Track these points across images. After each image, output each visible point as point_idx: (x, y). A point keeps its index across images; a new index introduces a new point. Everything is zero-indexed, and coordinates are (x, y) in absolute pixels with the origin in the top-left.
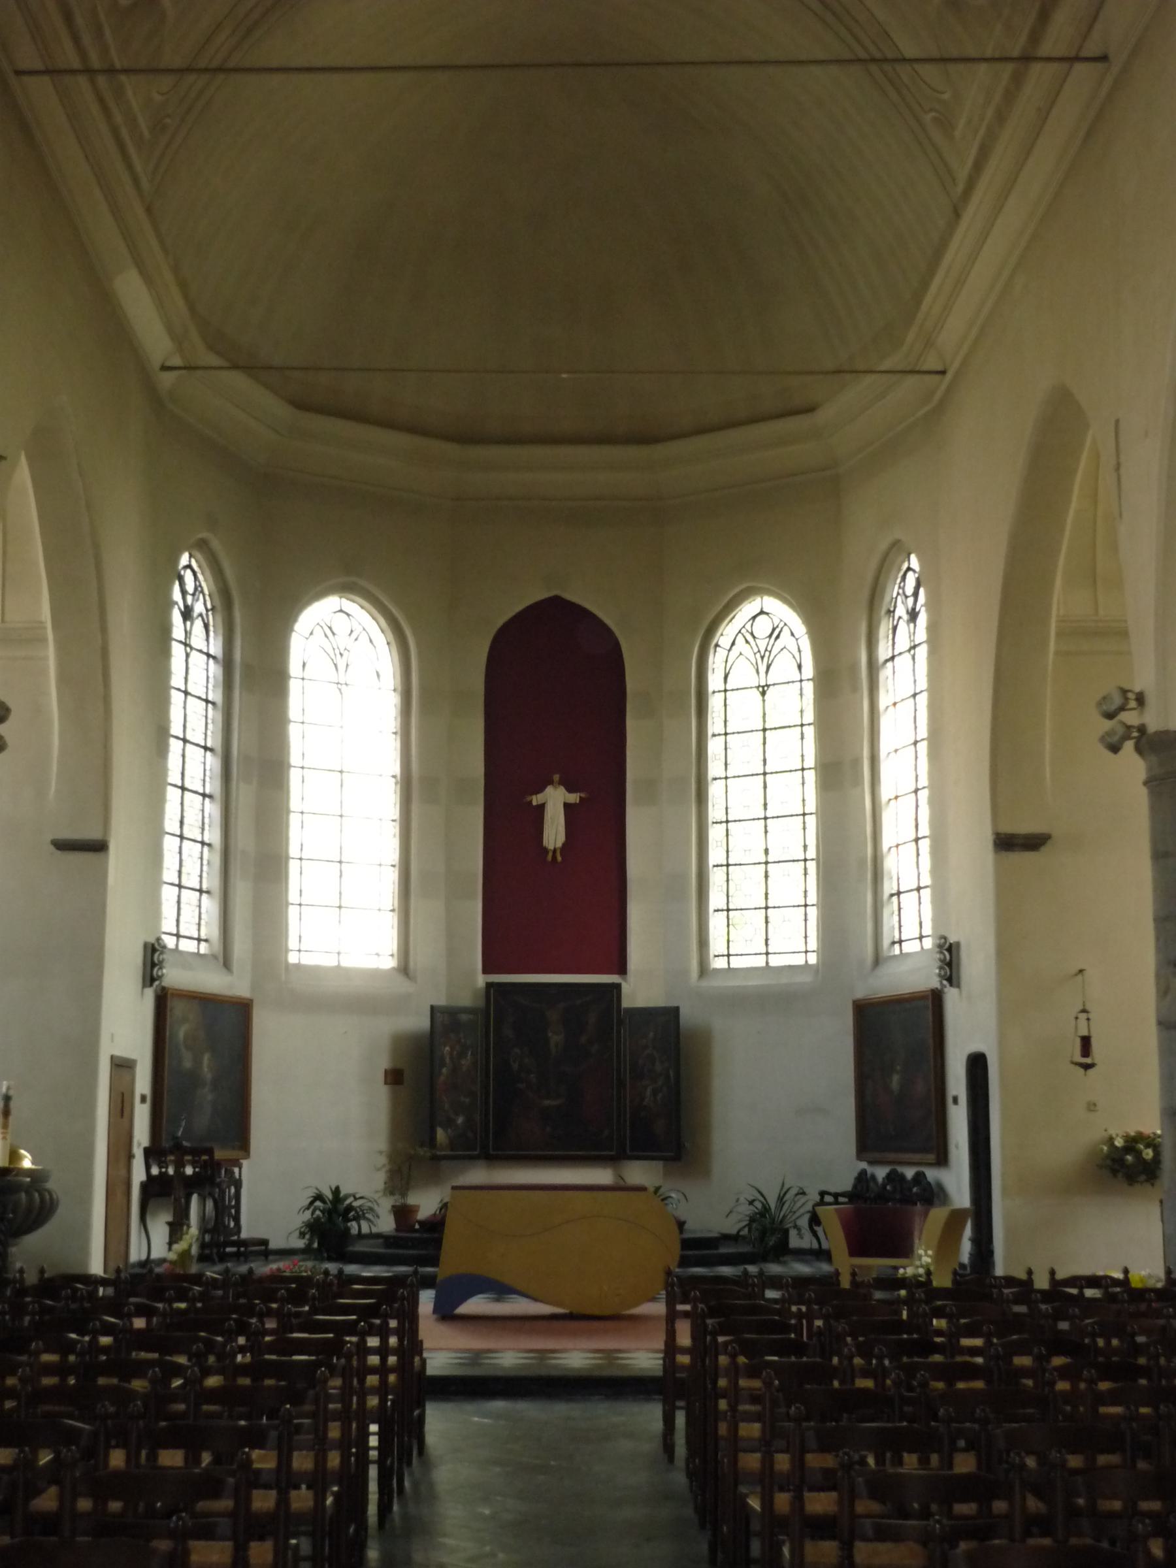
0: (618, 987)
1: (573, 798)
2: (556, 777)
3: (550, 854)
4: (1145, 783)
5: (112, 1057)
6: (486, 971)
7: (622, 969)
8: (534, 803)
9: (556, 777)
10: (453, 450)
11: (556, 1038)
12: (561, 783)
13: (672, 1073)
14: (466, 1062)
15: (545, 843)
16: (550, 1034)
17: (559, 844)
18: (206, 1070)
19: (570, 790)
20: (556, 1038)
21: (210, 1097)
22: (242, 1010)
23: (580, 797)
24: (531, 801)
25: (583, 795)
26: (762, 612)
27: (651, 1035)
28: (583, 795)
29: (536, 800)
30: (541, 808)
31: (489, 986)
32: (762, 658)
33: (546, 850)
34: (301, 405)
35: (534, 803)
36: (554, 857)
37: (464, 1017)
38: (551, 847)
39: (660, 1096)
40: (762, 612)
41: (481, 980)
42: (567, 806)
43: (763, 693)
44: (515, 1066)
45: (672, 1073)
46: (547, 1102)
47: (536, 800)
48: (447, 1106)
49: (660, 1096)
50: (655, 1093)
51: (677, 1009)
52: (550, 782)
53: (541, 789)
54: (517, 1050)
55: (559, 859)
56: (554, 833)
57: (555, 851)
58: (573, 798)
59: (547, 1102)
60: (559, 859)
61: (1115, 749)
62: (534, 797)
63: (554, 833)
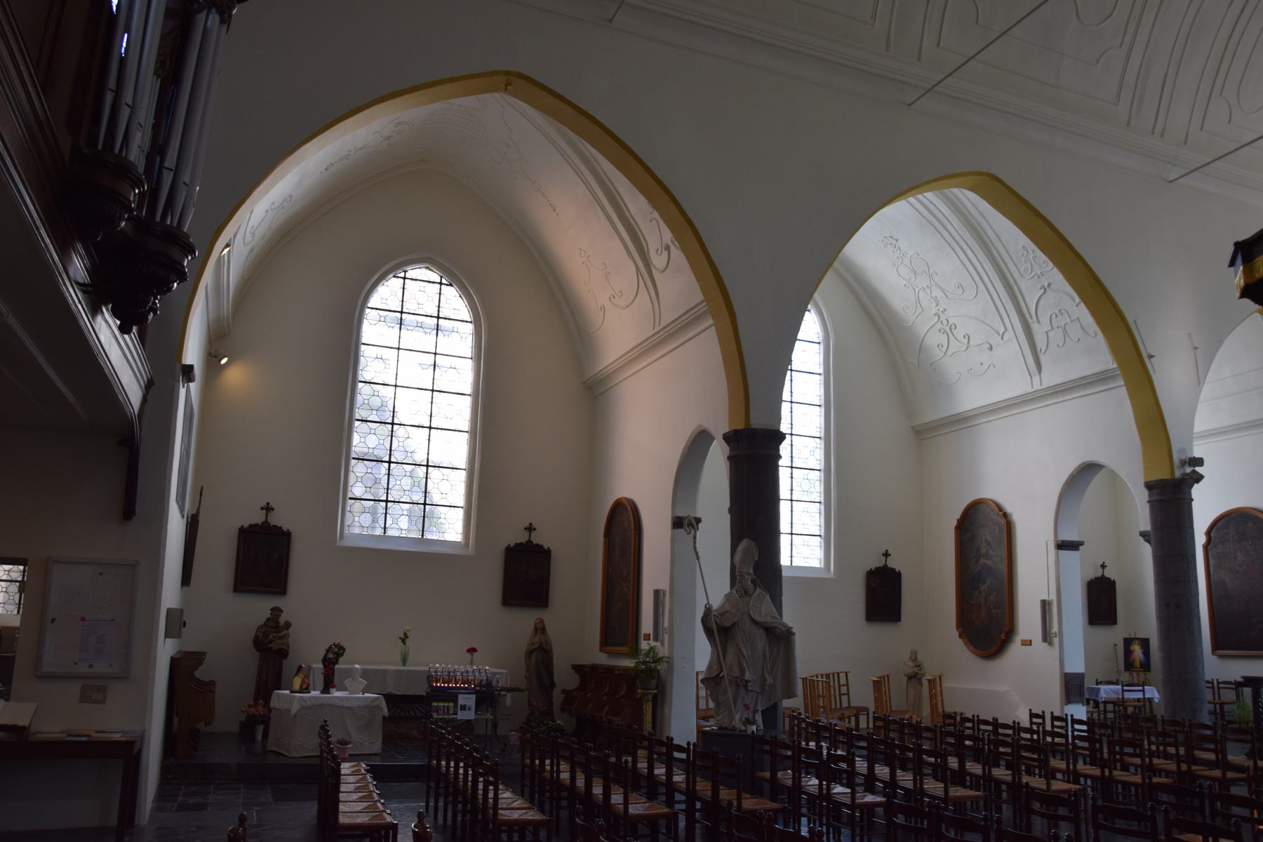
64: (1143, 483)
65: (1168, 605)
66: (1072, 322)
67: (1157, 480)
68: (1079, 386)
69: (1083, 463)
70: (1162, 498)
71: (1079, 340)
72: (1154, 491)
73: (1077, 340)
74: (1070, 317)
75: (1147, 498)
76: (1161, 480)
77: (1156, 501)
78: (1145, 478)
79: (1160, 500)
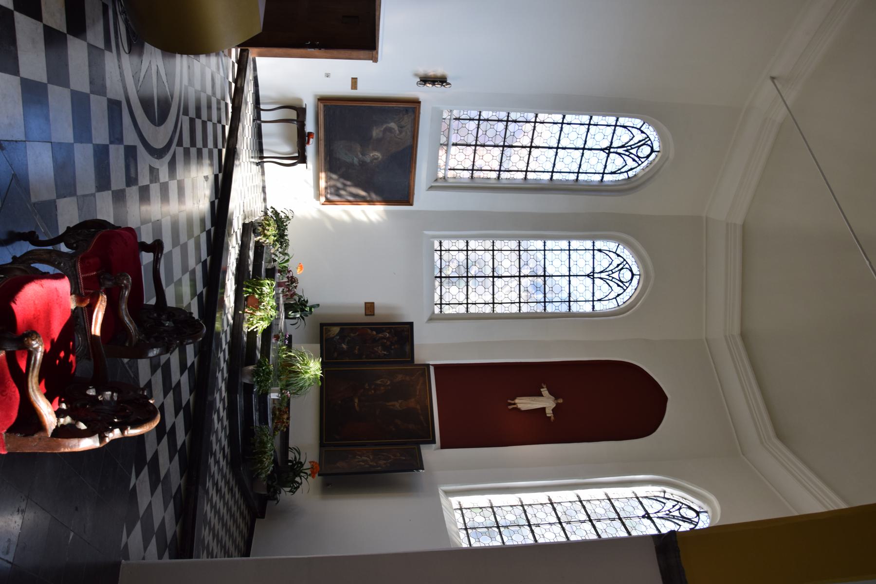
0: (434, 442)
1: (549, 413)
2: (560, 401)
3: (513, 402)
5: (375, 60)
6: (437, 367)
7: (444, 446)
8: (542, 390)
9: (560, 401)
10: (736, 331)
12: (558, 404)
16: (400, 401)
17: (520, 406)
18: (371, 155)
21: (356, 161)
22: (407, 200)
23: (550, 417)
24: (543, 388)
25: (552, 418)
29: (545, 391)
30: (540, 395)
32: (667, 514)
33: (514, 399)
34: (744, 226)
35: (542, 390)
37: (407, 348)
38: (517, 401)
39: (361, 463)
42: (544, 409)
44: (379, 382)
46: (356, 401)
47: (545, 391)
49: (361, 463)
50: (363, 461)
52: (556, 398)
53: (550, 393)
54: (389, 383)
55: (510, 407)
56: (525, 403)
57: (515, 404)
58: (549, 413)
59: (356, 401)
60: (510, 407)
62: (545, 389)
63: (525, 403)
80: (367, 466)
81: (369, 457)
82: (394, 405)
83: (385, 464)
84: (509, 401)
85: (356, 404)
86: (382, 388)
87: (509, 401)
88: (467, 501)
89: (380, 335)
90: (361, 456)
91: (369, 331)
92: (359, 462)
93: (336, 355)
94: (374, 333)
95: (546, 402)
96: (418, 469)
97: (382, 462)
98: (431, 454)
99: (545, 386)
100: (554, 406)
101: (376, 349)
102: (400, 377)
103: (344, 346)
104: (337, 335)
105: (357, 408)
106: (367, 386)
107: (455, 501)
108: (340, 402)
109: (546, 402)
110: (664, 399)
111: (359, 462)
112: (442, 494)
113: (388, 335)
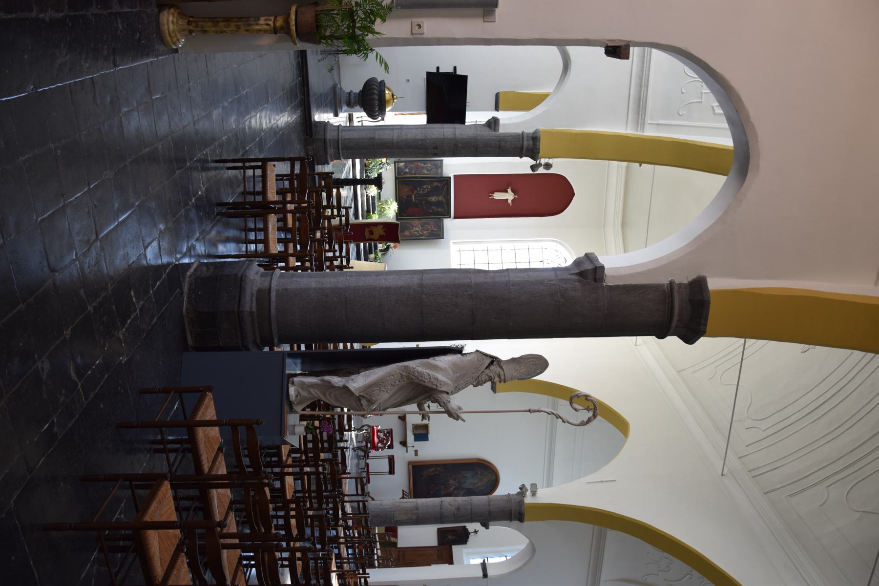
0: (450, 217)
1: (510, 202)
2: (517, 197)
4: (509, 494)
6: (454, 175)
7: (455, 217)
8: (508, 190)
9: (517, 197)
11: (433, 199)
12: (515, 198)
13: (424, 237)
14: (425, 171)
15: (495, 193)
16: (435, 197)
17: (495, 198)
19: (512, 201)
20: (433, 199)
24: (508, 188)
25: (511, 205)
26: (566, 261)
27: (435, 230)
28: (511, 205)
29: (509, 190)
30: (507, 192)
31: (450, 178)
33: (493, 193)
36: (491, 196)
38: (494, 195)
39: (416, 233)
40: (566, 261)
41: (451, 175)
42: (507, 199)
43: (541, 262)
44: (424, 187)
45: (424, 237)
46: (413, 197)
47: (509, 190)
48: (411, 166)
49: (416, 233)
50: (417, 231)
51: (443, 238)
52: (515, 195)
53: (513, 191)
54: (430, 187)
56: (498, 196)
58: (510, 202)
59: (413, 197)
60: (490, 198)
61: (520, 489)
63: (498, 196)
64: (541, 128)
65: (436, 148)
66: (702, 93)
67: (539, 149)
68: (642, 71)
69: (570, 60)
70: (524, 149)
71: (683, 93)
72: (531, 143)
73: (683, 91)
74: (705, 93)
75: (526, 131)
76: (539, 152)
77: (523, 144)
78: (545, 132)
79: (522, 148)
80: (418, 235)
81: (419, 228)
82: (431, 199)
83: (427, 233)
84: (491, 195)
85: (413, 199)
86: (426, 190)
87: (491, 195)
88: (463, 247)
89: (426, 165)
90: (415, 227)
91: (420, 164)
92: (415, 231)
93: (402, 174)
94: (423, 165)
95: (509, 196)
96: (441, 238)
97: (425, 232)
98: (450, 224)
99: (510, 188)
100: (513, 198)
101: (423, 171)
102: (436, 184)
103: (407, 170)
104: (404, 165)
105: (414, 201)
106: (418, 189)
107: (457, 247)
108: (405, 197)
109: (509, 196)
110: (573, 194)
111: (415, 231)
112: (451, 244)
113: (429, 165)
